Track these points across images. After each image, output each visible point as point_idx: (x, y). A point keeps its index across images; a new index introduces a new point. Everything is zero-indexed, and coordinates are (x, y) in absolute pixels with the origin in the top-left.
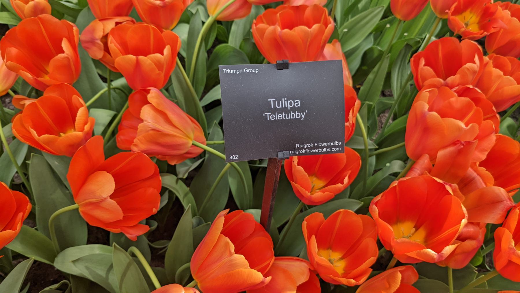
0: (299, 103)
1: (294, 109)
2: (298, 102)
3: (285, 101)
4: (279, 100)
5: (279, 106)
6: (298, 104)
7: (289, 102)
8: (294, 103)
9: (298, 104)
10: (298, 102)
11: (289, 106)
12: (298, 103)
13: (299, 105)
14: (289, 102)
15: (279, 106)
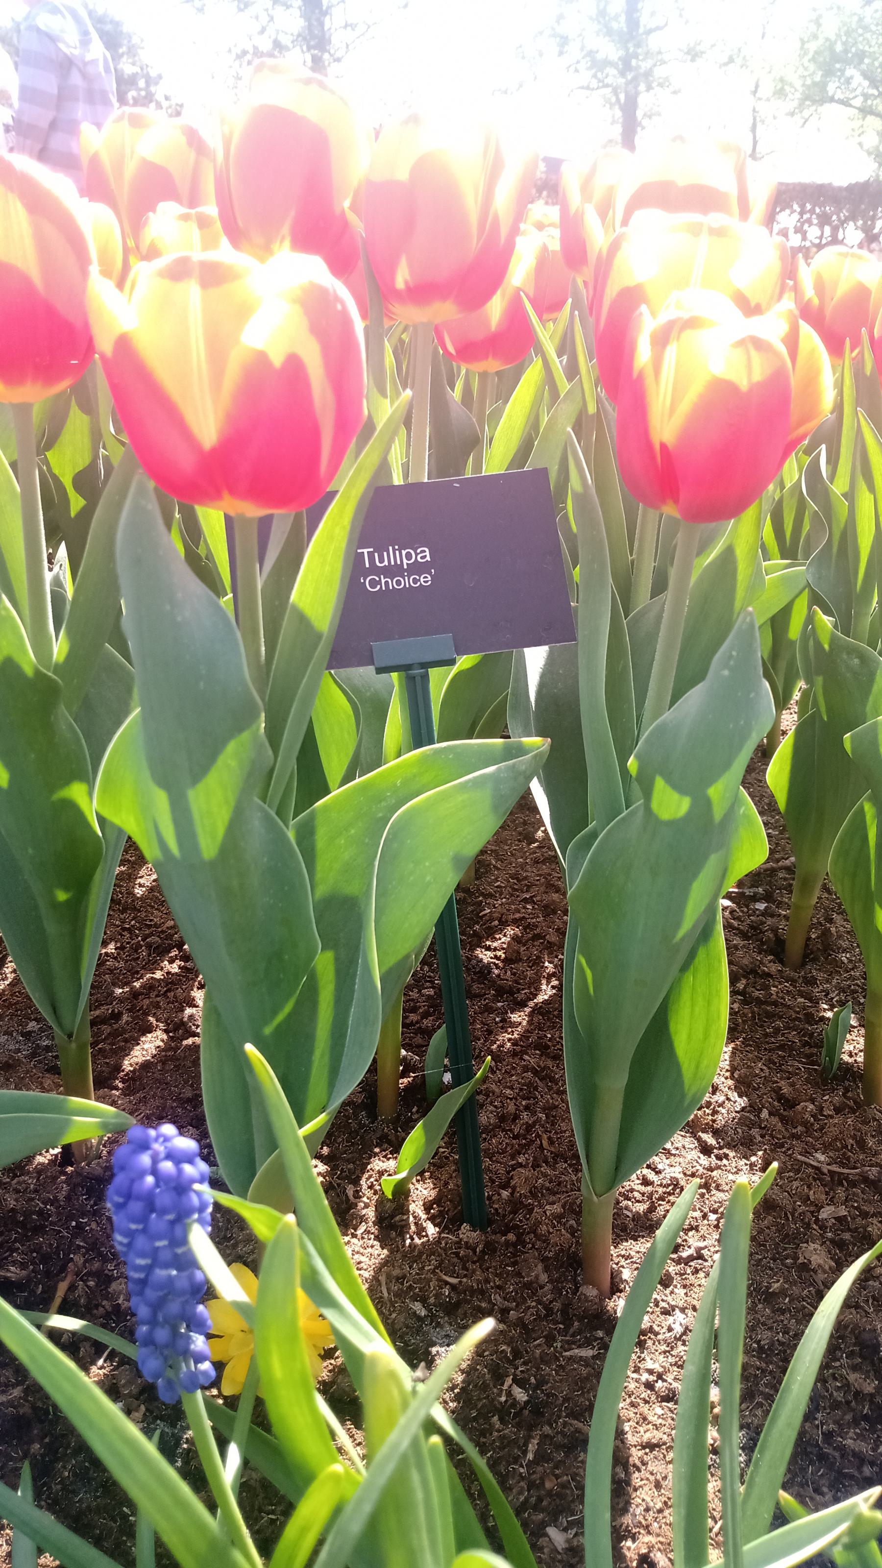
0: (427, 553)
1: (417, 568)
2: (425, 551)
3: (394, 550)
4: (381, 549)
5: (381, 561)
6: (425, 556)
7: (404, 553)
8: (417, 555)
9: (425, 556)
10: (425, 551)
11: (405, 561)
12: (425, 554)
13: (428, 558)
14: (404, 553)
15: (381, 561)
